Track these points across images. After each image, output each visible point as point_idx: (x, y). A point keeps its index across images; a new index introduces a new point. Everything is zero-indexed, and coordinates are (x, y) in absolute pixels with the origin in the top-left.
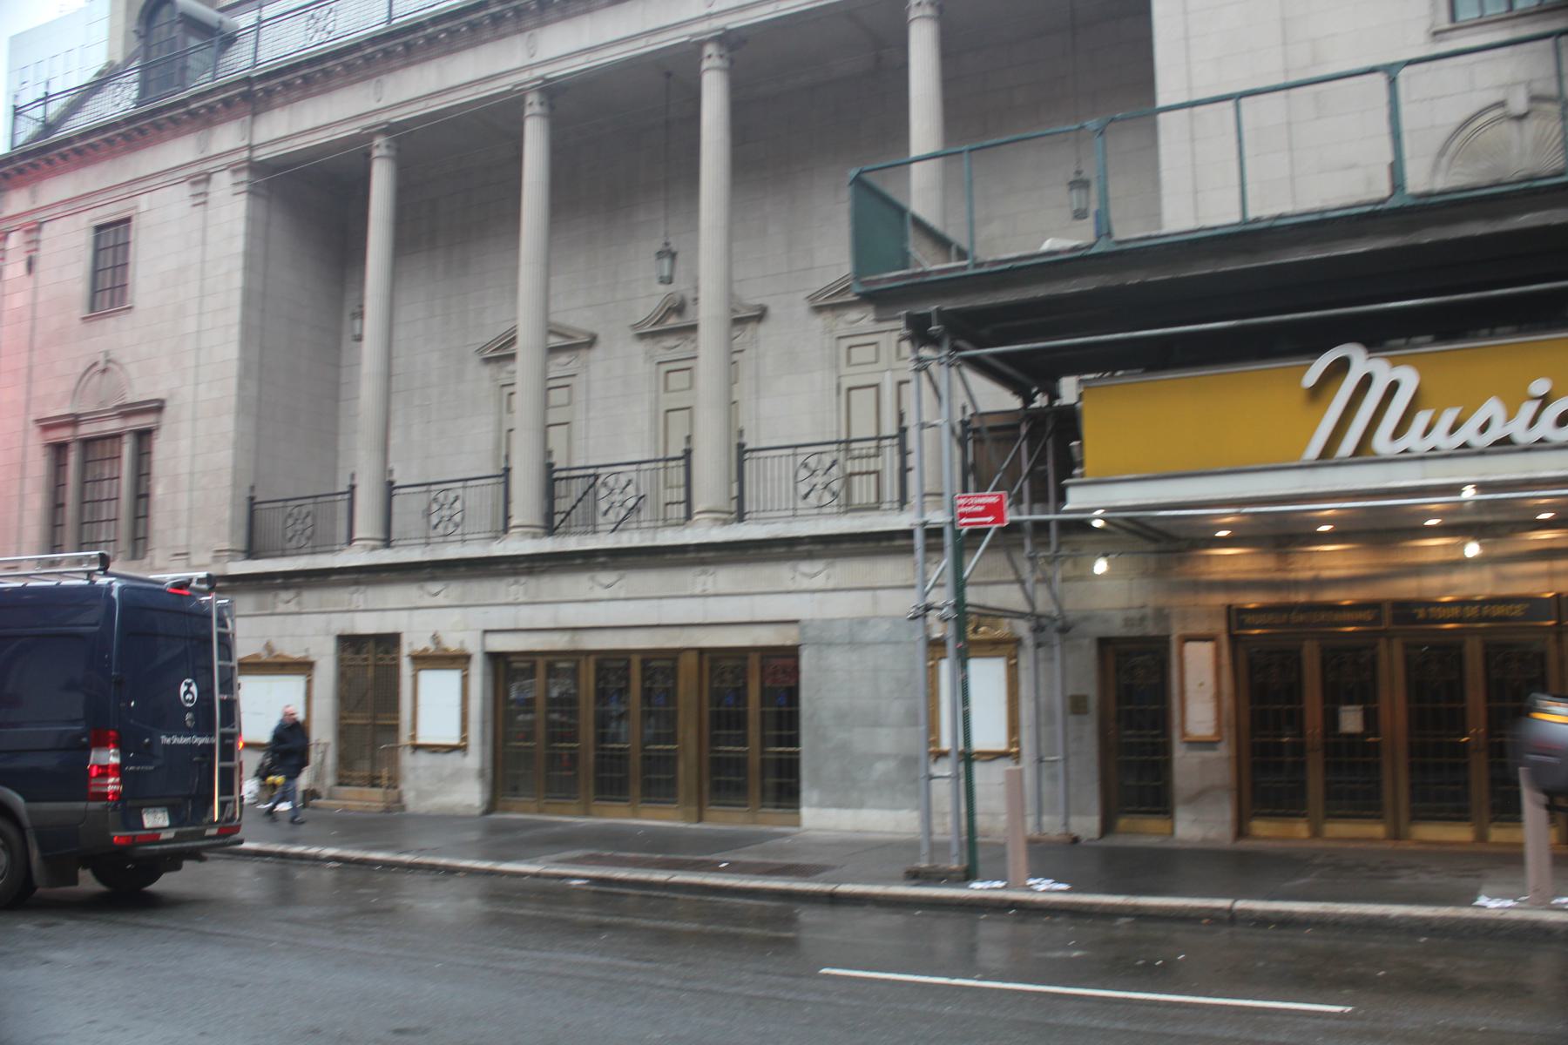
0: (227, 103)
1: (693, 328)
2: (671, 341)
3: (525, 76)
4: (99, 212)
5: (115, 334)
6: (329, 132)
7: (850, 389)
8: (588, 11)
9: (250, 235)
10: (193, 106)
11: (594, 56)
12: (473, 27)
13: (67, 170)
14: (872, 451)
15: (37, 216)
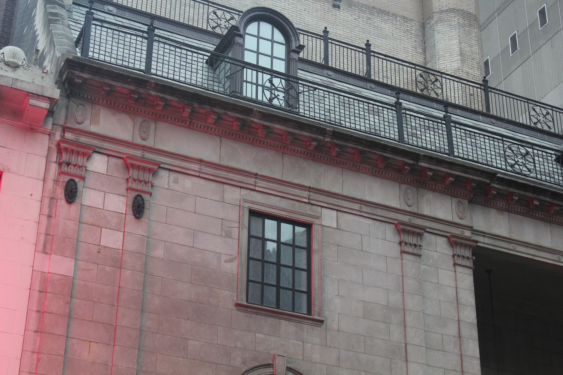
0: (457, 177)
4: (258, 197)
5: (281, 339)
6: (556, 257)
10: (422, 164)
13: (207, 130)
15: (148, 155)
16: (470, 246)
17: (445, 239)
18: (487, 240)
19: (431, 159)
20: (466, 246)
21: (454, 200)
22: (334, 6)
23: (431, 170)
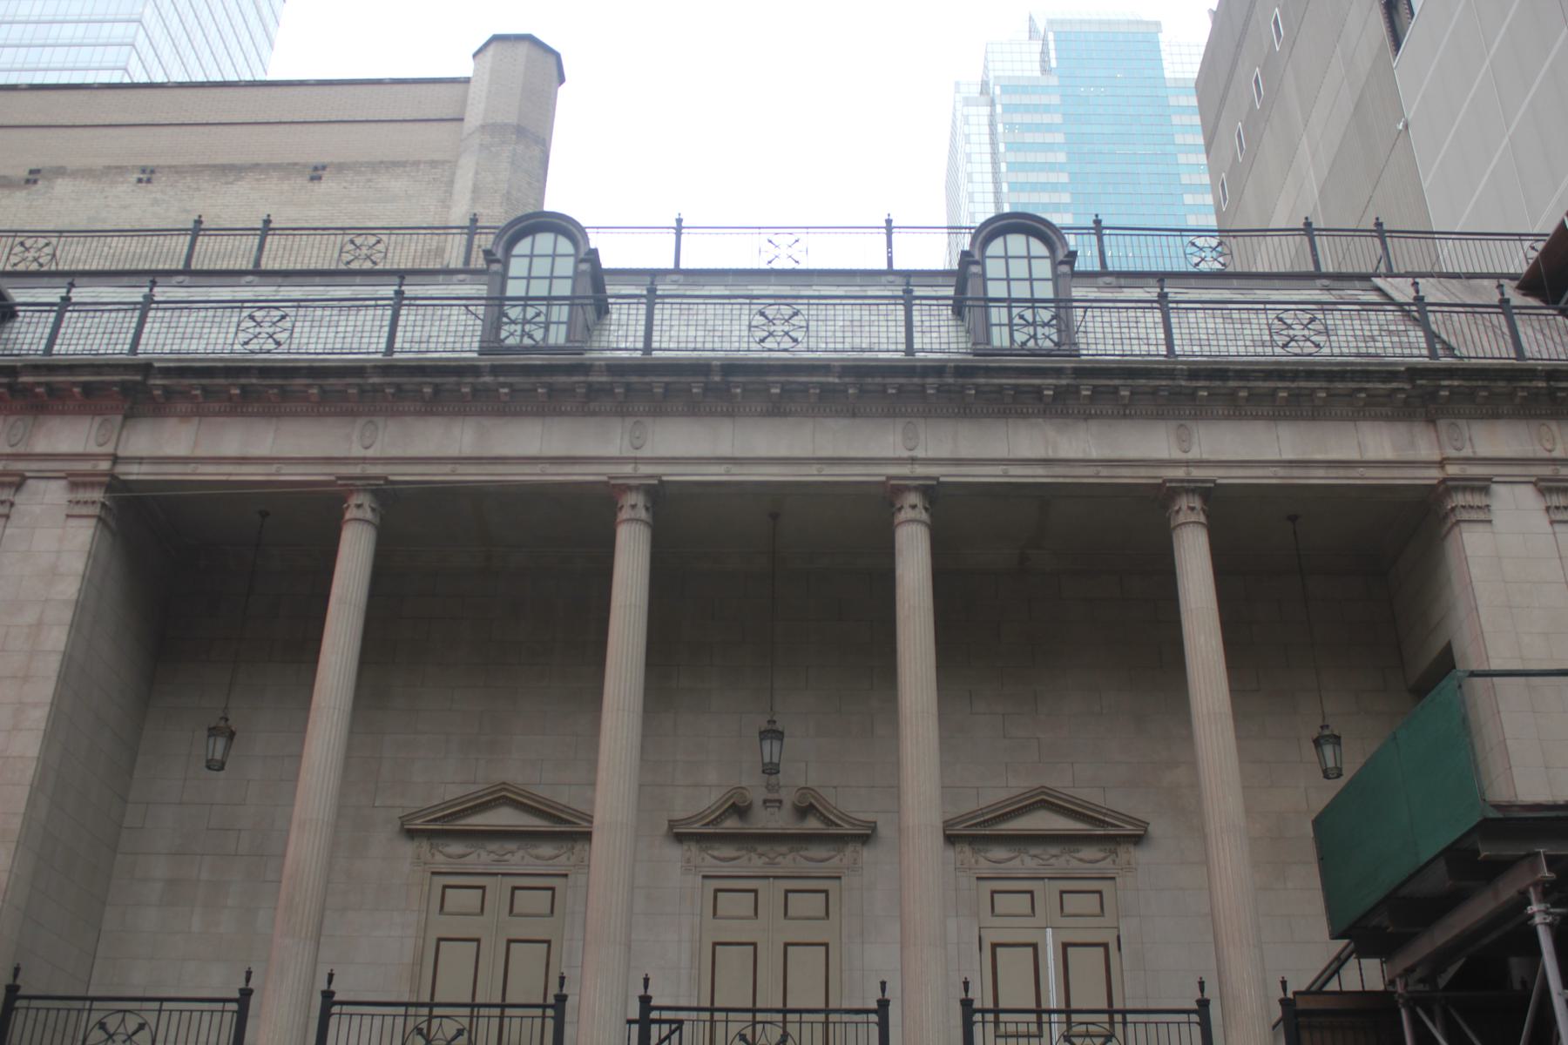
1: (587, 836)
2: (727, 851)
3: (628, 469)
6: (273, 468)
7: (994, 946)
8: (730, 414)
9: (87, 580)
11: (735, 469)
12: (552, 391)
14: (1022, 1028)
16: (100, 484)
17: (63, 483)
18: (145, 468)
19: (36, 368)
20: (92, 485)
21: (98, 419)
22: (312, 179)
23: (39, 384)
